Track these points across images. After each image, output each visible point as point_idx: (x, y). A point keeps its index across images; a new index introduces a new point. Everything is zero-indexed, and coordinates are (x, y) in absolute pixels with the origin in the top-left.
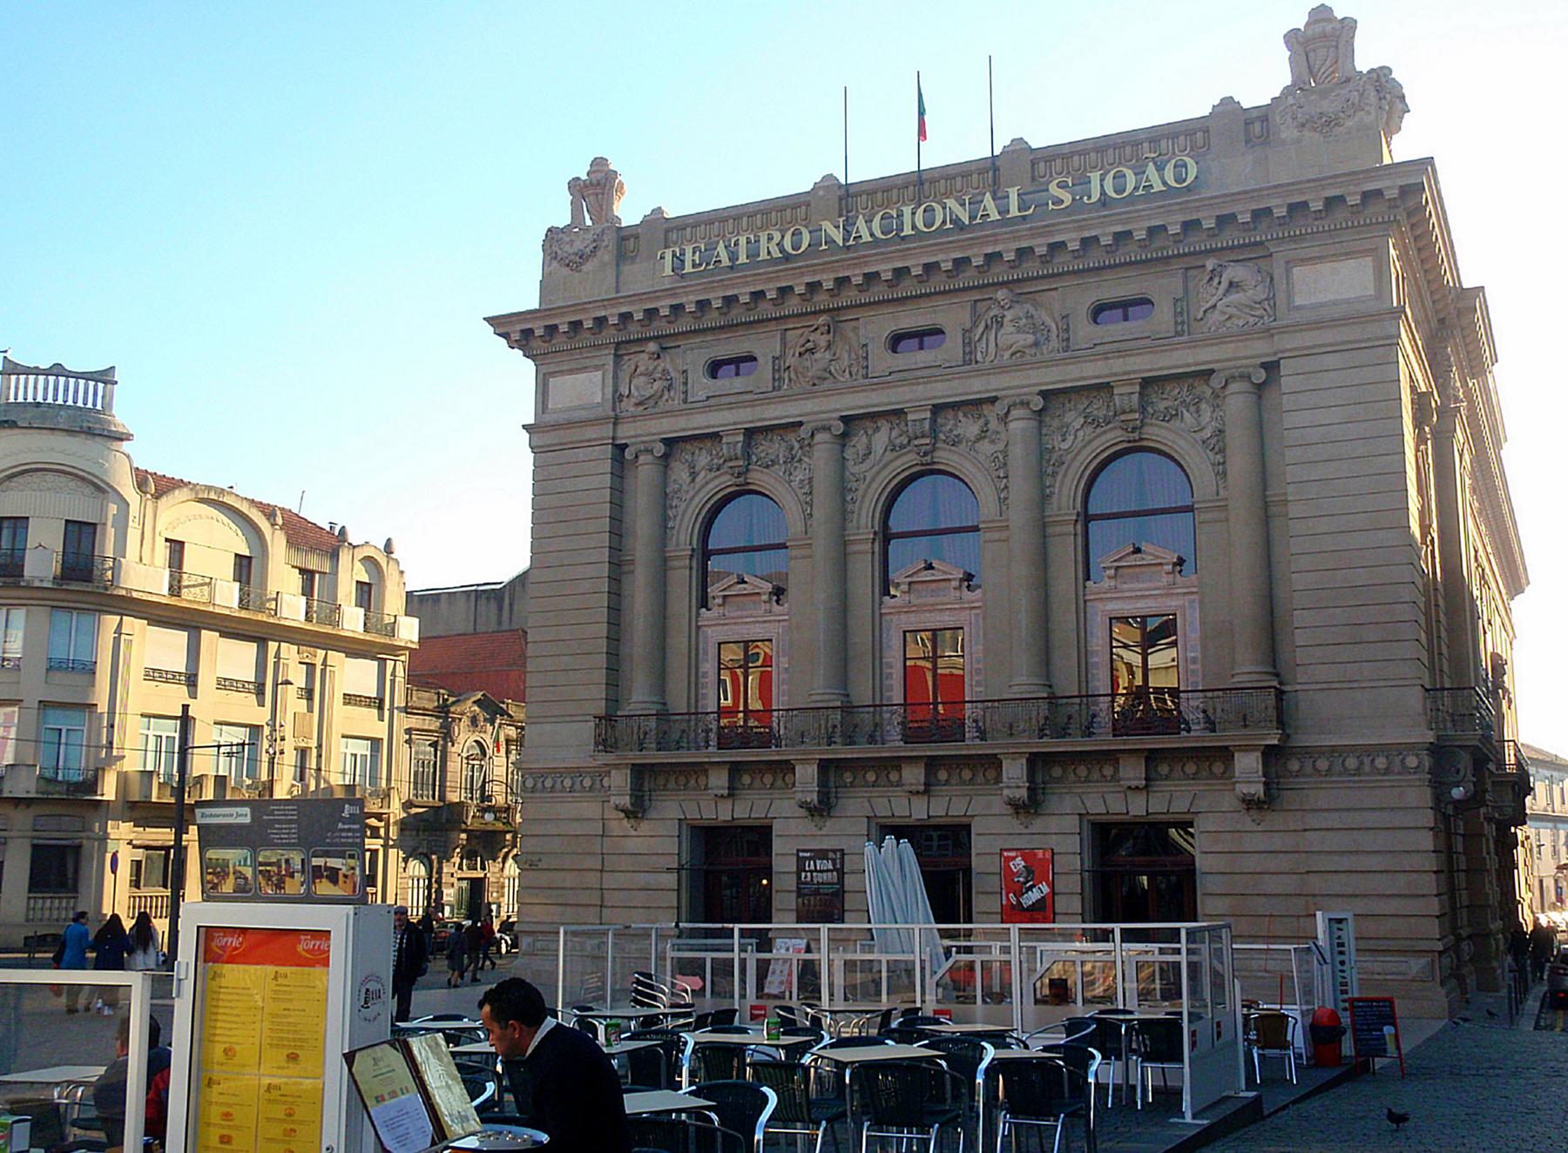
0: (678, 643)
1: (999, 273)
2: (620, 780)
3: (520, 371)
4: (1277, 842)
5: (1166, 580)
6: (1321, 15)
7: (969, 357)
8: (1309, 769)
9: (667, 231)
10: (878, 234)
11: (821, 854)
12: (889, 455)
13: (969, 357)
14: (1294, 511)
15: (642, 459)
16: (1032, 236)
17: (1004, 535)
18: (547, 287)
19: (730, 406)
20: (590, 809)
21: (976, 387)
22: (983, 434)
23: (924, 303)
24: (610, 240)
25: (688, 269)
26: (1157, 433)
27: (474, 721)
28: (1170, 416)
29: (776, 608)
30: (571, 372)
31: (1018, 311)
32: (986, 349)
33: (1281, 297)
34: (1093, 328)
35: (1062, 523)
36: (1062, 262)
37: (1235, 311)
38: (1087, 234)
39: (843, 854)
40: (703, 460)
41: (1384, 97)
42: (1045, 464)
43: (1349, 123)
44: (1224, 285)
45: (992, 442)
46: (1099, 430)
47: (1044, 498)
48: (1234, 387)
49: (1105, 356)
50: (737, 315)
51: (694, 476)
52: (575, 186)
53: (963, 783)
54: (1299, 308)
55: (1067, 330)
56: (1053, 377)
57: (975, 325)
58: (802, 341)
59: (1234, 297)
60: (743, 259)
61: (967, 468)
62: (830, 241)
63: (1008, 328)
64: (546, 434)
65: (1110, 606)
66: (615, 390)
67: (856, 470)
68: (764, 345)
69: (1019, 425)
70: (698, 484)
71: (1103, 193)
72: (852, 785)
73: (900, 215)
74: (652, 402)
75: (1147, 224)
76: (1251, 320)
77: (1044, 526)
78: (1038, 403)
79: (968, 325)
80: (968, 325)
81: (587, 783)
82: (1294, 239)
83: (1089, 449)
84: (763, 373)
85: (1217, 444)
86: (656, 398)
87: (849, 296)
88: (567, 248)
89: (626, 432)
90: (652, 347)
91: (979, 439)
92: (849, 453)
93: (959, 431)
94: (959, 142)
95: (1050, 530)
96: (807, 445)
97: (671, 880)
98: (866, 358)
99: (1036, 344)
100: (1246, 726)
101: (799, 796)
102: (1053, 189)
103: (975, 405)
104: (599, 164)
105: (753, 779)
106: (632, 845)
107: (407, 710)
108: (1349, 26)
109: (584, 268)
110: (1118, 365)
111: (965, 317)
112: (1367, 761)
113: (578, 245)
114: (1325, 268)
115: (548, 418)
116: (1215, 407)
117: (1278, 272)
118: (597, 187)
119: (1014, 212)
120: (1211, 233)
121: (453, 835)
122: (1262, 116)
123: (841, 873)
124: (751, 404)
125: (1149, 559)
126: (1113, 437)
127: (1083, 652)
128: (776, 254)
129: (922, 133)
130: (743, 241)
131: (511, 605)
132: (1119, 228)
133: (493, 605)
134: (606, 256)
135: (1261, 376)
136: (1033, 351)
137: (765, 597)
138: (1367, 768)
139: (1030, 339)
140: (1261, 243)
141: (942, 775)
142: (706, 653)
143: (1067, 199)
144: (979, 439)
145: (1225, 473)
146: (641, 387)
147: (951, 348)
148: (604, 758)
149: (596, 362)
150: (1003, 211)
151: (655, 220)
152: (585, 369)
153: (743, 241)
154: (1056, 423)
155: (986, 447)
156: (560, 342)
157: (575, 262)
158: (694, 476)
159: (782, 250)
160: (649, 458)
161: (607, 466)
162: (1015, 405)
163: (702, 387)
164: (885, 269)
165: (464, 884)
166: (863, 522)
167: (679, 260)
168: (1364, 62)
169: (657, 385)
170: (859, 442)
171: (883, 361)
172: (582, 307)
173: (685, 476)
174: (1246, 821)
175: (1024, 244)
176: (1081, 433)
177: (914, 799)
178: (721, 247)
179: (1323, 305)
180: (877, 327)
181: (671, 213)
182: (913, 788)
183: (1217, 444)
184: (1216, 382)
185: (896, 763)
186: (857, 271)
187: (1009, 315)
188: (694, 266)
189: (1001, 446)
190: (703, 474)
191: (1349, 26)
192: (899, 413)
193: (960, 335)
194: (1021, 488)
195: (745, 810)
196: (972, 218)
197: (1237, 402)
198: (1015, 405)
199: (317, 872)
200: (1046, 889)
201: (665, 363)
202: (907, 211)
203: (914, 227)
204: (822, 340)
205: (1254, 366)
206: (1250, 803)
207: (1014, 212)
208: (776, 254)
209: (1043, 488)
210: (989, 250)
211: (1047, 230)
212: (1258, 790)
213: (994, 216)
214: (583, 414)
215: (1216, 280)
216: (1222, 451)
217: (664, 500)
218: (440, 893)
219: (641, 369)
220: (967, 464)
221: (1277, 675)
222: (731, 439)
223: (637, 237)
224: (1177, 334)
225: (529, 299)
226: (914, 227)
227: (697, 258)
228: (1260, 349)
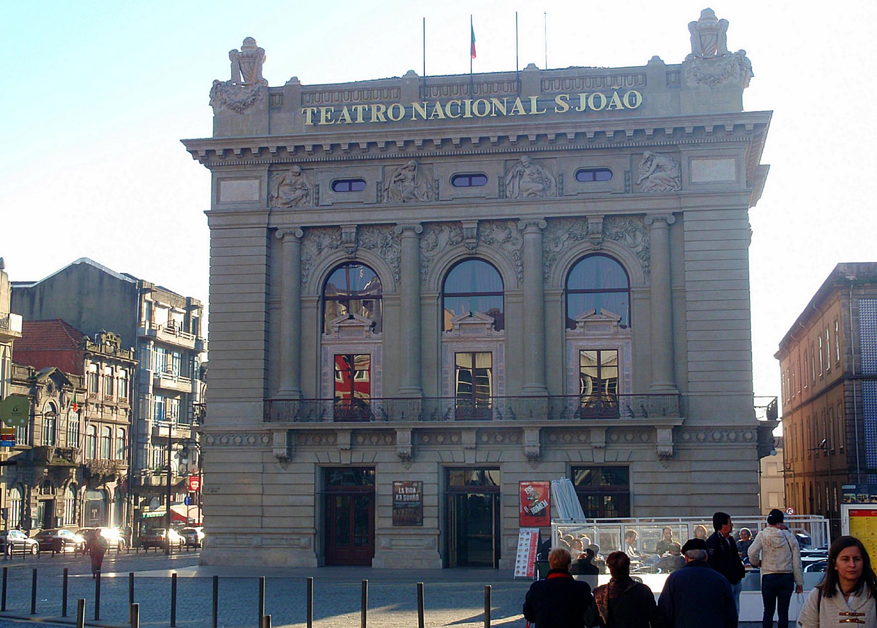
0: (310, 354)
1: (523, 146)
2: (280, 439)
3: (202, 176)
4: (676, 478)
5: (613, 330)
6: (708, 14)
7: (502, 195)
8: (694, 438)
9: (302, 94)
10: (449, 114)
11: (410, 484)
12: (449, 248)
13: (502, 195)
14: (689, 297)
15: (287, 238)
16: (547, 129)
17: (520, 299)
18: (218, 122)
19: (349, 210)
21: (508, 212)
22: (508, 239)
23: (474, 159)
24: (263, 96)
25: (323, 122)
26: (610, 246)
27: (50, 388)
28: (618, 237)
29: (373, 335)
30: (236, 178)
31: (533, 169)
32: (513, 188)
33: (685, 177)
34: (576, 183)
35: (555, 294)
36: (561, 144)
37: (658, 181)
38: (579, 131)
39: (423, 484)
40: (326, 241)
41: (740, 68)
42: (546, 259)
43: (725, 82)
44: (654, 167)
45: (514, 244)
46: (577, 242)
47: (545, 279)
48: (657, 225)
49: (585, 200)
50: (355, 154)
51: (320, 250)
52: (233, 54)
53: (497, 442)
54: (694, 184)
55: (562, 183)
56: (553, 210)
57: (506, 174)
58: (396, 174)
59: (658, 174)
60: (360, 120)
61: (497, 259)
62: (418, 115)
63: (526, 178)
64: (220, 218)
65: (580, 343)
66: (269, 193)
67: (427, 254)
68: (371, 174)
69: (531, 236)
70: (323, 256)
71: (587, 106)
72: (428, 443)
73: (463, 104)
74: (293, 203)
75: (614, 129)
76: (668, 187)
77: (544, 295)
78: (543, 224)
79: (502, 174)
80: (502, 174)
81: (252, 440)
82: (694, 145)
83: (570, 253)
84: (370, 192)
85: (646, 255)
86: (297, 200)
87: (430, 150)
88: (232, 97)
89: (276, 221)
90: (296, 168)
92: (423, 244)
93: (493, 236)
94: (495, 61)
95: (547, 298)
96: (398, 238)
97: (310, 500)
98: (438, 188)
99: (543, 189)
100: (664, 415)
101: (399, 450)
102: (558, 100)
103: (502, 222)
104: (249, 42)
105: (364, 440)
106: (282, 479)
107: (12, 381)
108: (724, 24)
109: (245, 112)
110: (591, 206)
111: (500, 169)
112: (725, 434)
113: (241, 97)
114: (710, 162)
115: (221, 207)
116: (644, 235)
117: (684, 162)
118: (248, 58)
119: (534, 111)
120: (650, 137)
121: (39, 469)
122: (677, 70)
123: (422, 496)
124: (363, 210)
125: (603, 318)
126: (585, 246)
127: (565, 370)
128: (383, 119)
129: (473, 53)
130: (360, 108)
131: (41, 300)
132: (598, 129)
133: (26, 300)
134: (262, 106)
135: (672, 220)
136: (541, 194)
137: (367, 328)
138: (725, 438)
139: (541, 187)
141: (485, 438)
142: (326, 361)
143: (566, 107)
145: (649, 272)
146: (285, 193)
147: (492, 187)
148: (268, 426)
149: (255, 174)
150: (528, 109)
151: (294, 85)
152: (246, 178)
153: (360, 108)
154: (552, 236)
155: (509, 247)
156: (231, 159)
157: (240, 108)
158: (320, 250)
159: (386, 117)
160: (292, 238)
161: (264, 241)
162: (530, 224)
163: (328, 196)
164: (456, 138)
165: (42, 504)
166: (432, 286)
167: (316, 116)
168: (733, 46)
169: (299, 193)
170: (430, 237)
171: (447, 191)
172: (253, 140)
173: (314, 250)
174: (659, 466)
175: (542, 132)
176: (566, 243)
177: (467, 452)
178: (345, 111)
179: (708, 183)
180: (445, 170)
181: (306, 80)
182: (468, 446)
183: (646, 255)
184: (647, 221)
185: (458, 431)
186: (438, 137)
187: (528, 171)
188: (327, 120)
189: (518, 247)
190: (326, 250)
191: (724, 24)
192: (456, 224)
193: (497, 180)
194: (532, 272)
195: (357, 458)
196: (508, 111)
197: (658, 233)
198: (530, 224)
199: (872, 498)
200: (546, 504)
201: (302, 179)
202: (468, 102)
203: (472, 113)
204: (410, 175)
205: (669, 214)
206: (664, 457)
207: (534, 111)
208: (383, 119)
209: (544, 273)
210: (521, 133)
211: (556, 126)
212: (669, 450)
213: (522, 112)
214: (248, 207)
215: (649, 163)
216: (648, 259)
217: (300, 264)
218: (29, 510)
219: (287, 181)
220: (498, 257)
221: (675, 386)
222: (347, 230)
223: (281, 95)
224: (626, 191)
225: (205, 130)
226: (472, 113)
227: (329, 116)
228: (673, 205)
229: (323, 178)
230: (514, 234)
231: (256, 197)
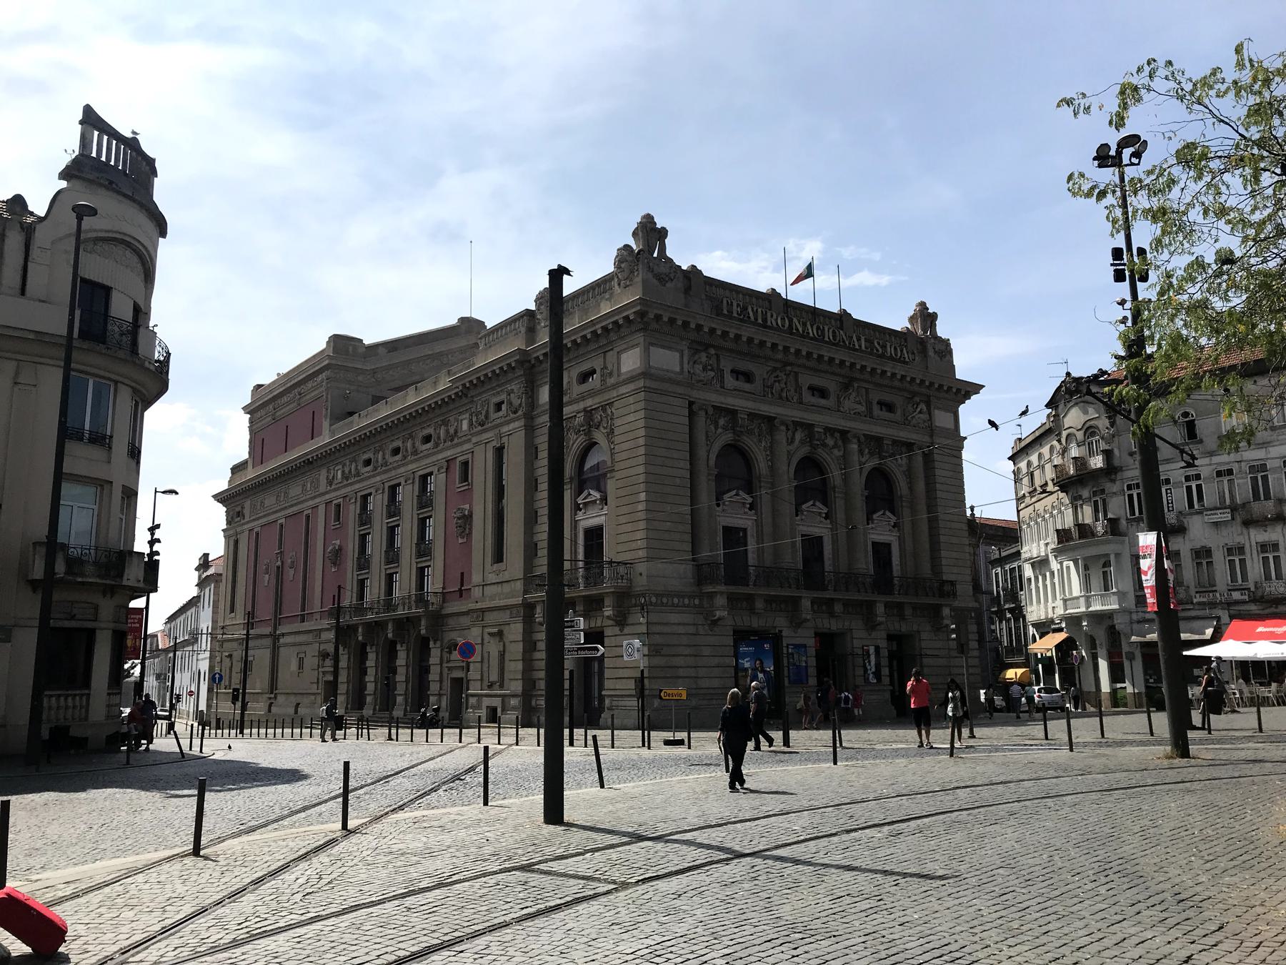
20: (687, 618)
30: (663, 347)
51: (716, 428)
68: (759, 371)
90: (712, 351)
91: (834, 447)
118: (651, 233)
140: (929, 396)
144: (834, 447)
155: (836, 452)
161: (686, 412)
190: (720, 430)
197: (919, 460)
229: (727, 365)
230: (840, 443)
231: (678, 369)
